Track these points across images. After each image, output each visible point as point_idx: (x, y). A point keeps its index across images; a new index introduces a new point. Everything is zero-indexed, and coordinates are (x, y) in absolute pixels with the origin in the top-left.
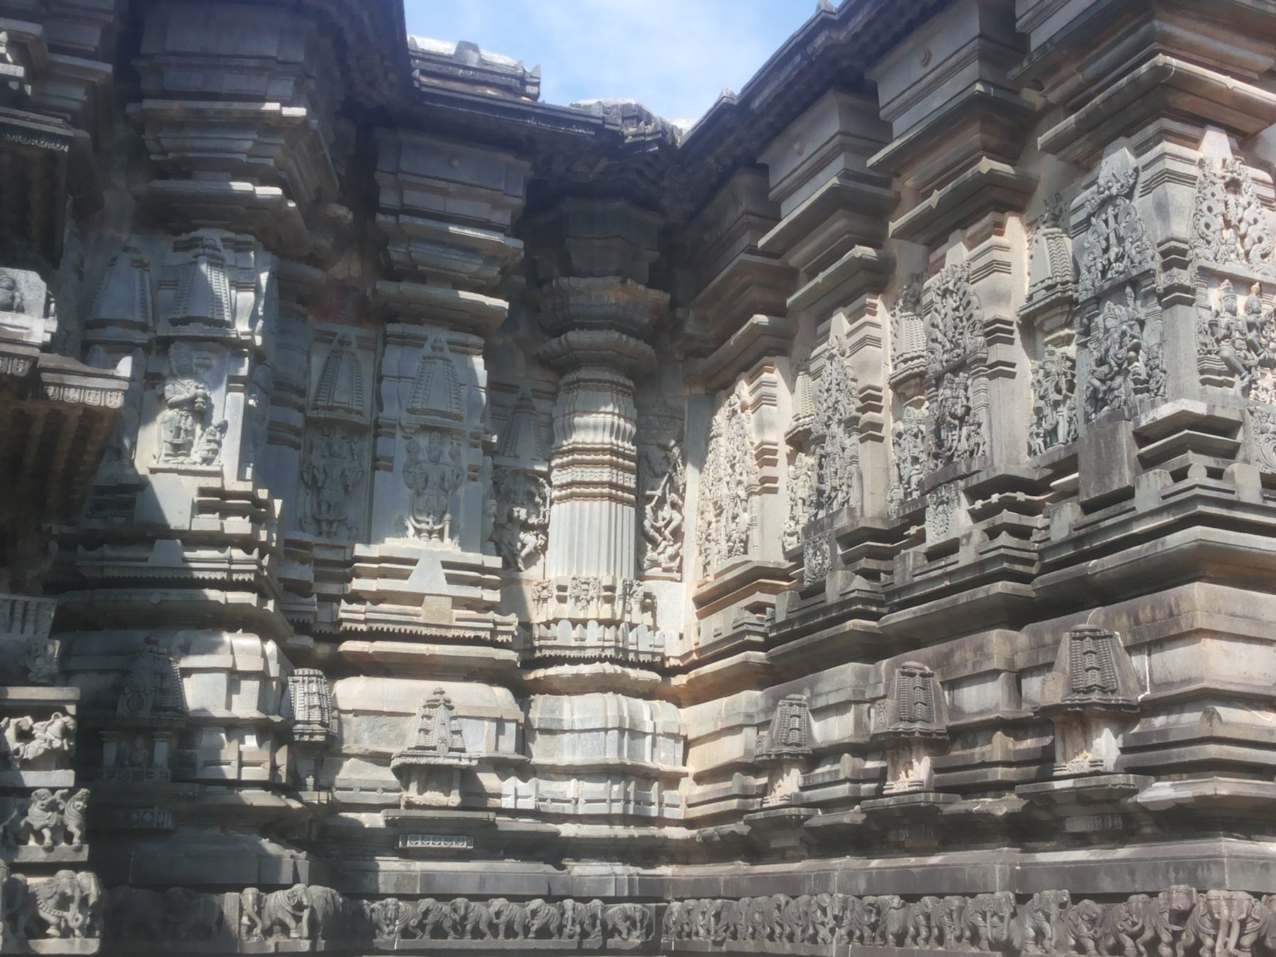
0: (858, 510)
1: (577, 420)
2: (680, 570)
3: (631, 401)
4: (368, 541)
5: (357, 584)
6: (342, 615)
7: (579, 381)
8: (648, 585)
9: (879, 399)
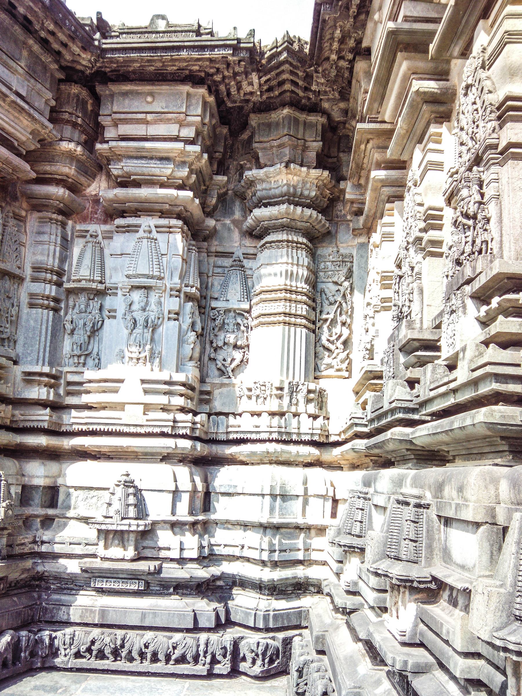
0: (418, 321)
1: (263, 271)
2: (349, 370)
3: (304, 253)
4: (98, 366)
5: (85, 399)
6: (73, 420)
7: (267, 243)
8: (323, 384)
9: (441, 218)
